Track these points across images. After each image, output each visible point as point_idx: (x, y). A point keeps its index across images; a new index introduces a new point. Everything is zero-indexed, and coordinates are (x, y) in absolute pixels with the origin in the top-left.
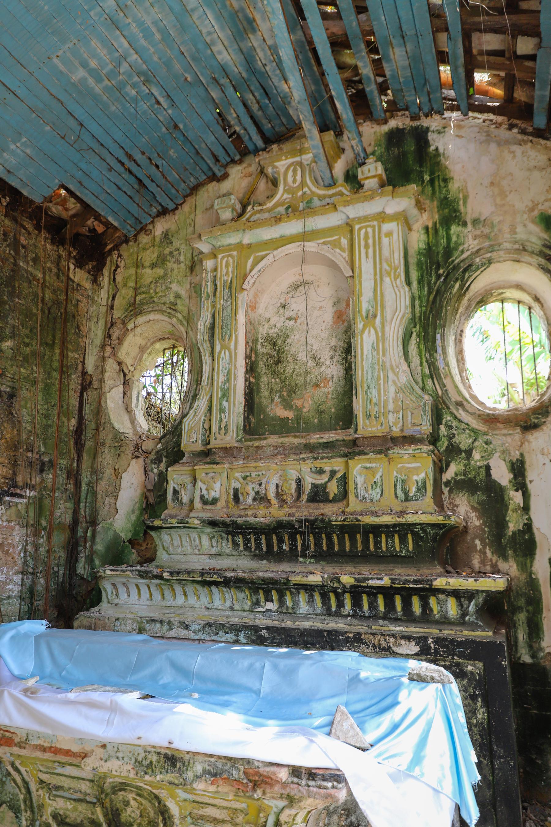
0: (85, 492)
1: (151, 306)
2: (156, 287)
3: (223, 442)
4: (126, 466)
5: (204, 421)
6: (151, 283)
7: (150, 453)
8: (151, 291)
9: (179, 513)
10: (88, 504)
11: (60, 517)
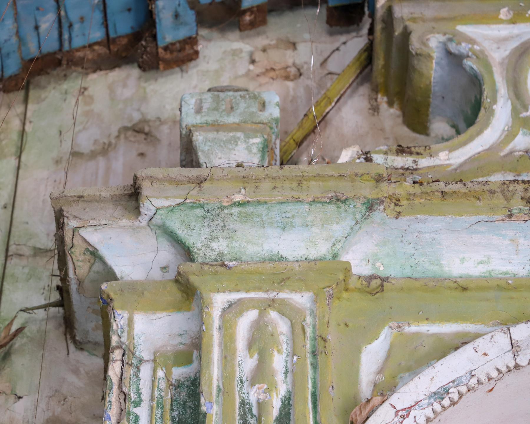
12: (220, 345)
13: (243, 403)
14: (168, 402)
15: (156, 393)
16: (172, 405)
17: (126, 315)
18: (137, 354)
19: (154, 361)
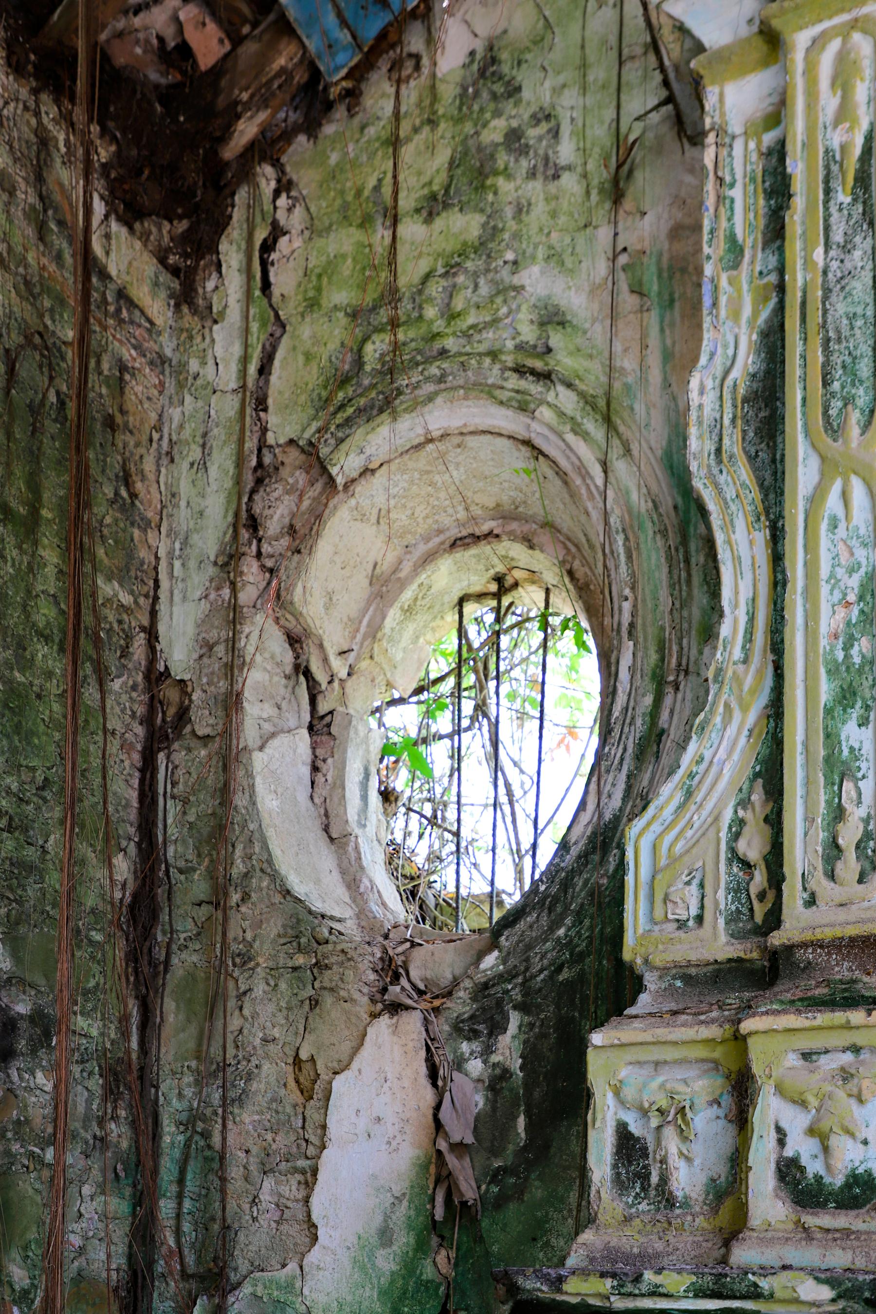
0: (177, 1153)
1: (434, 370)
2: (451, 292)
3: (854, 914)
4: (346, 1047)
5: (738, 827)
6: (427, 277)
7: (450, 994)
8: (430, 312)
9: (659, 1246)
10: (187, 1204)
11: (82, 1251)
12: (804, 93)
13: (827, 151)
14: (760, 175)
15: (749, 168)
16: (763, 176)
17: (716, 89)
18: (730, 131)
19: (746, 133)
